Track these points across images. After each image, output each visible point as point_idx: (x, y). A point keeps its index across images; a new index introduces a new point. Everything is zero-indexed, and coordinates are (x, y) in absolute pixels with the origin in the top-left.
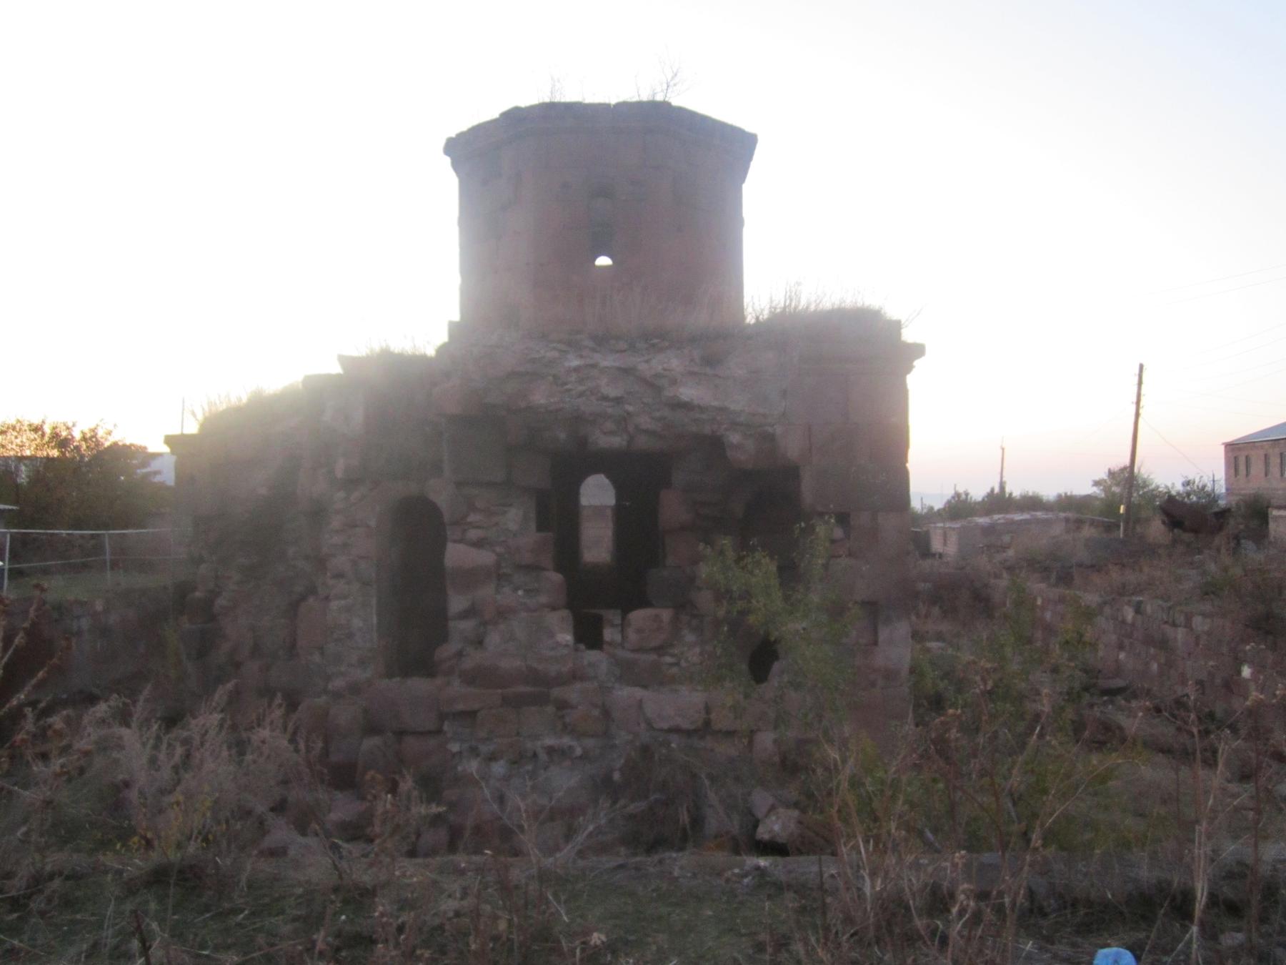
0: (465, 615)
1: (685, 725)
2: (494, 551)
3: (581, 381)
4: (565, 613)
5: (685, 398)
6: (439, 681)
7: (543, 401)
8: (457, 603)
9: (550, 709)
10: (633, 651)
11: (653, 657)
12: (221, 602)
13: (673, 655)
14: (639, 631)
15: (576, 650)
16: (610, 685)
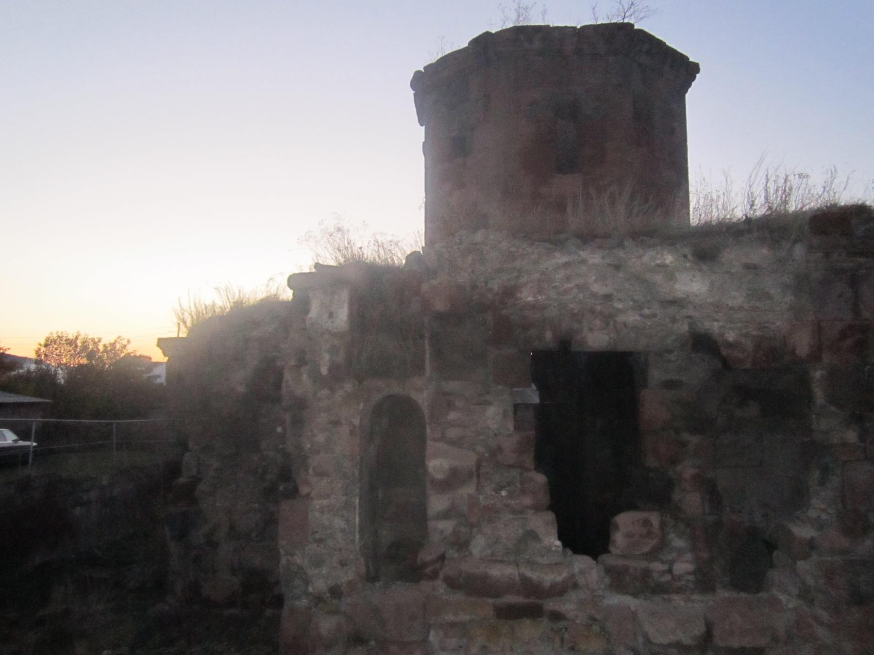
0: (445, 515)
1: (687, 641)
2: (474, 450)
3: (568, 279)
4: (550, 516)
5: (679, 295)
6: (426, 586)
7: (530, 299)
8: (437, 503)
9: (545, 622)
10: (624, 556)
11: (643, 564)
12: (202, 487)
13: (663, 562)
14: (629, 535)
15: (564, 554)
16: (600, 593)
